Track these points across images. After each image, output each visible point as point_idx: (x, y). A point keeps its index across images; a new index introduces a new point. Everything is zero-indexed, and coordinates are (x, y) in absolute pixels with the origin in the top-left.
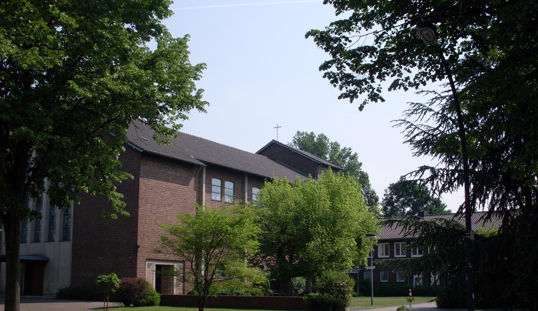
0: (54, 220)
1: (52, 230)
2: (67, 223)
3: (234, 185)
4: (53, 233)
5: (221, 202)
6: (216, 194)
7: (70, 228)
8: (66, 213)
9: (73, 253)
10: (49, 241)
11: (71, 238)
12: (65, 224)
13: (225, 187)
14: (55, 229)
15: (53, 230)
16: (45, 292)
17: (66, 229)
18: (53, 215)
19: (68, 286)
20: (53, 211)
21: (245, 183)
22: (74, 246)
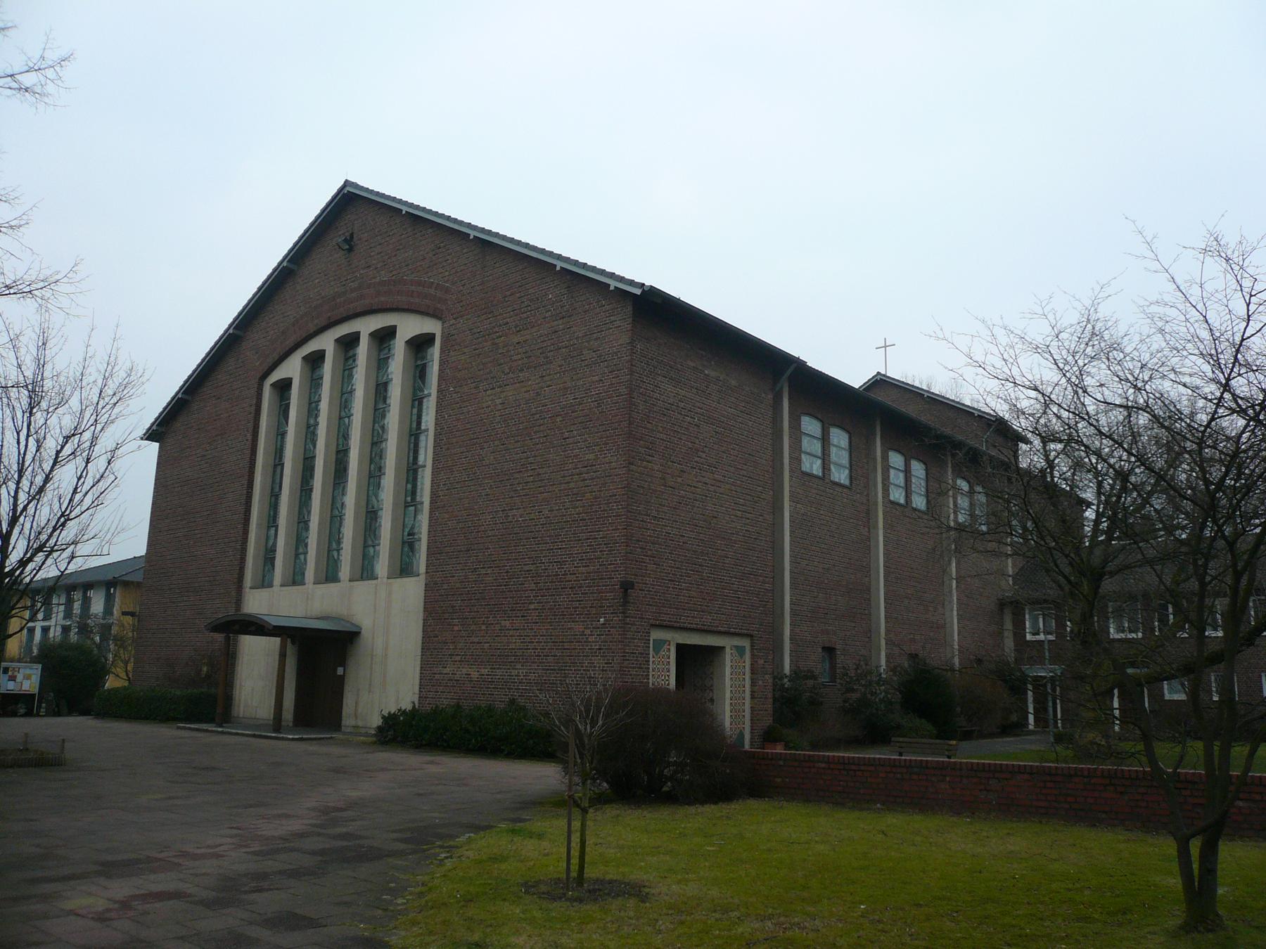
0: (379, 520)
1: (371, 550)
2: (413, 527)
3: (850, 438)
4: (373, 557)
5: (823, 478)
6: (812, 458)
7: (420, 540)
8: (409, 499)
9: (425, 609)
10: (362, 579)
11: (422, 569)
12: (407, 530)
13: (831, 442)
14: (379, 545)
15: (373, 546)
16: (348, 721)
17: (407, 543)
18: (375, 507)
19: (409, 707)
20: (376, 496)
21: (874, 435)
22: (430, 588)
